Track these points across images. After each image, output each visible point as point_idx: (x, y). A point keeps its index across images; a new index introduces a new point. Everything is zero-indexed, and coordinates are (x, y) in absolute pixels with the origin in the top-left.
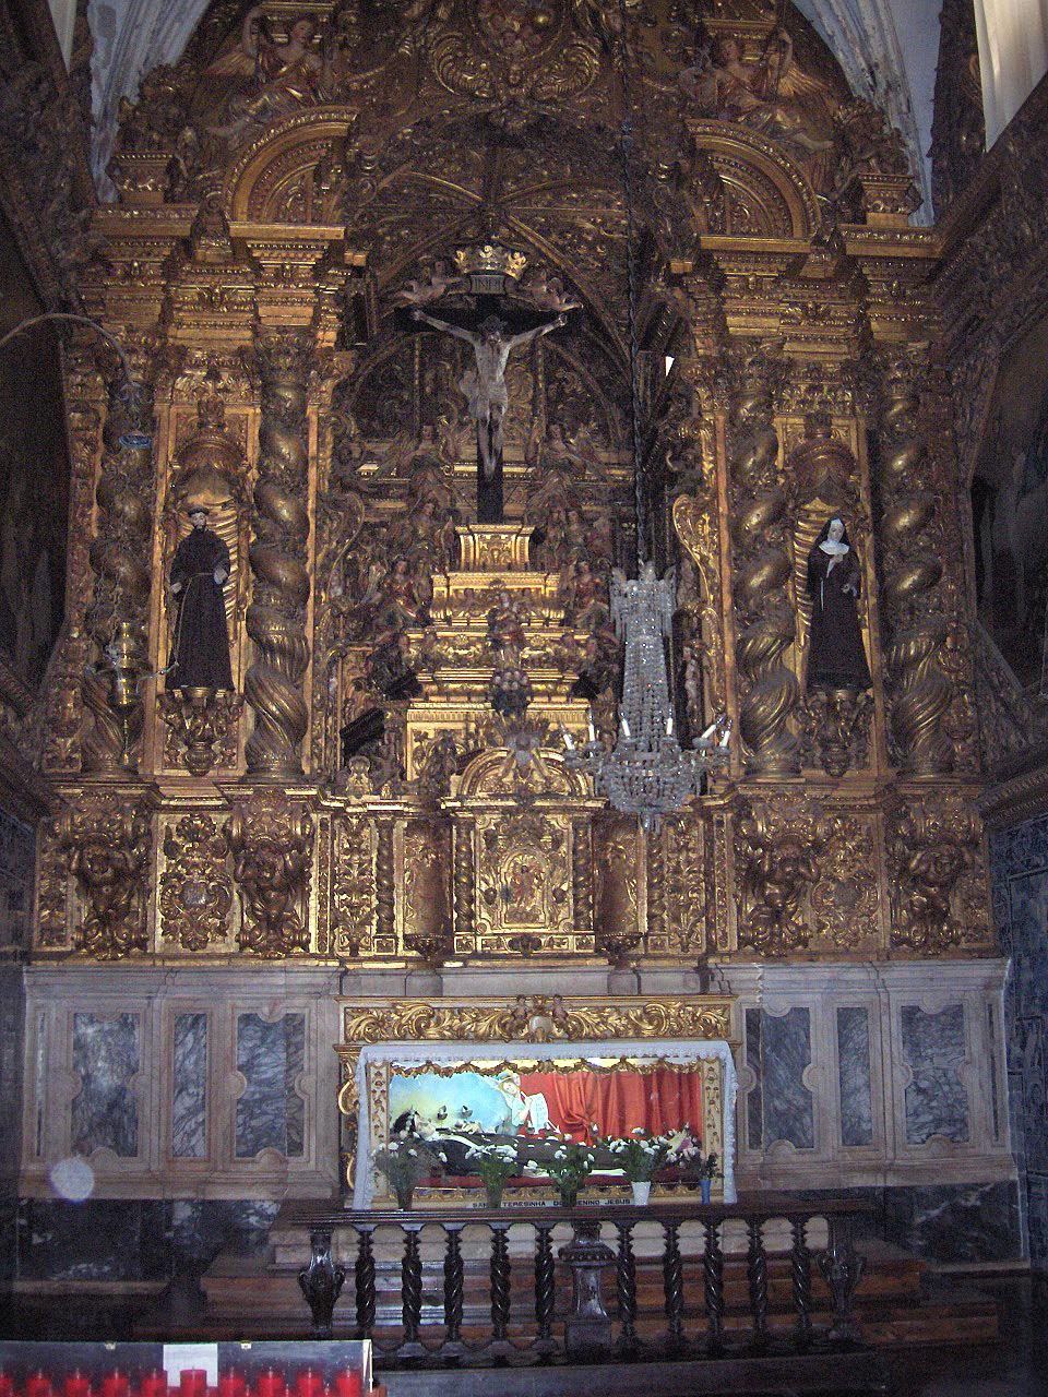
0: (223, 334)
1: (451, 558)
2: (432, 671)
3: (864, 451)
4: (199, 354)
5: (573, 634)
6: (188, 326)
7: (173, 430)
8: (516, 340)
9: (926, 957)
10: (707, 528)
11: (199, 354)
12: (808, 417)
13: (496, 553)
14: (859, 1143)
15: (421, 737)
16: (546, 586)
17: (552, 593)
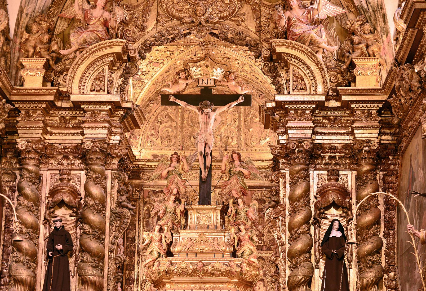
3: (354, 188)
7: (48, 182)
10: (281, 223)
12: (328, 171)
16: (225, 236)
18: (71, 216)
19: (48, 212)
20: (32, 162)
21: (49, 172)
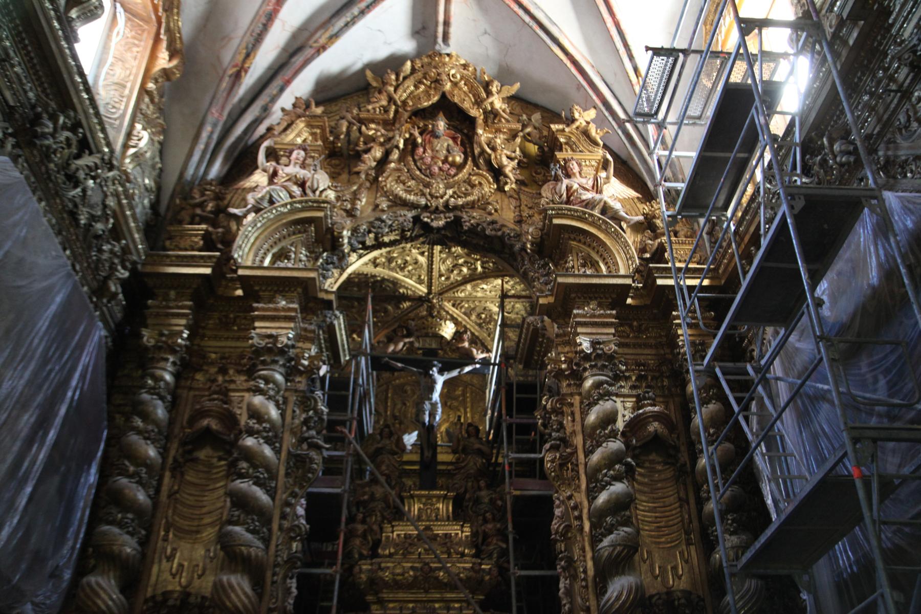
0: (233, 344)
1: (398, 515)
2: (376, 593)
4: (213, 356)
5: (481, 564)
6: (209, 338)
8: (447, 376)
11: (213, 356)
13: (429, 511)
16: (462, 532)
17: (467, 537)
18: (220, 459)
19: (181, 451)
20: (162, 364)
21: (192, 393)
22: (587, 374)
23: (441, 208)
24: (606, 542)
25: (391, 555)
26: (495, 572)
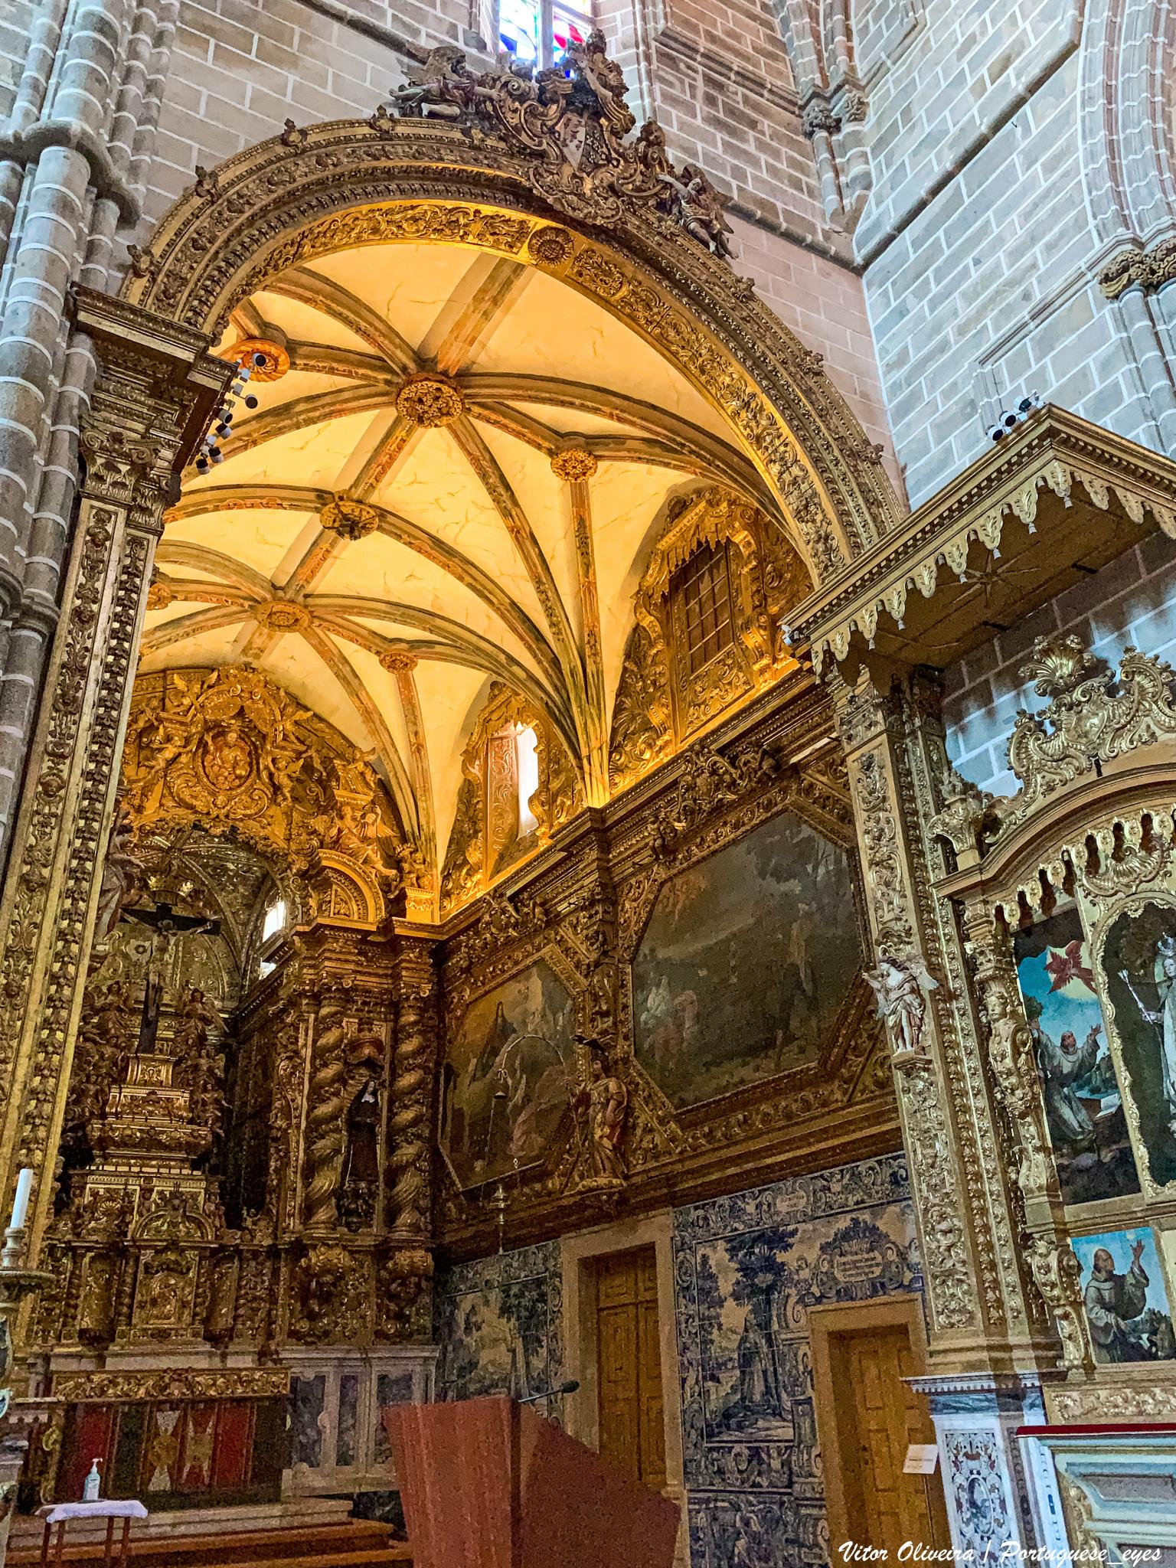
2: (103, 1149)
9: (394, 1343)
14: (346, 1464)
15: (95, 1194)
22: (325, 1002)
23: (222, 817)
24: (320, 1144)
25: (116, 1114)
26: (210, 1138)
